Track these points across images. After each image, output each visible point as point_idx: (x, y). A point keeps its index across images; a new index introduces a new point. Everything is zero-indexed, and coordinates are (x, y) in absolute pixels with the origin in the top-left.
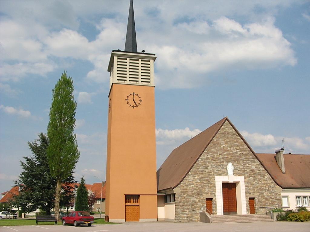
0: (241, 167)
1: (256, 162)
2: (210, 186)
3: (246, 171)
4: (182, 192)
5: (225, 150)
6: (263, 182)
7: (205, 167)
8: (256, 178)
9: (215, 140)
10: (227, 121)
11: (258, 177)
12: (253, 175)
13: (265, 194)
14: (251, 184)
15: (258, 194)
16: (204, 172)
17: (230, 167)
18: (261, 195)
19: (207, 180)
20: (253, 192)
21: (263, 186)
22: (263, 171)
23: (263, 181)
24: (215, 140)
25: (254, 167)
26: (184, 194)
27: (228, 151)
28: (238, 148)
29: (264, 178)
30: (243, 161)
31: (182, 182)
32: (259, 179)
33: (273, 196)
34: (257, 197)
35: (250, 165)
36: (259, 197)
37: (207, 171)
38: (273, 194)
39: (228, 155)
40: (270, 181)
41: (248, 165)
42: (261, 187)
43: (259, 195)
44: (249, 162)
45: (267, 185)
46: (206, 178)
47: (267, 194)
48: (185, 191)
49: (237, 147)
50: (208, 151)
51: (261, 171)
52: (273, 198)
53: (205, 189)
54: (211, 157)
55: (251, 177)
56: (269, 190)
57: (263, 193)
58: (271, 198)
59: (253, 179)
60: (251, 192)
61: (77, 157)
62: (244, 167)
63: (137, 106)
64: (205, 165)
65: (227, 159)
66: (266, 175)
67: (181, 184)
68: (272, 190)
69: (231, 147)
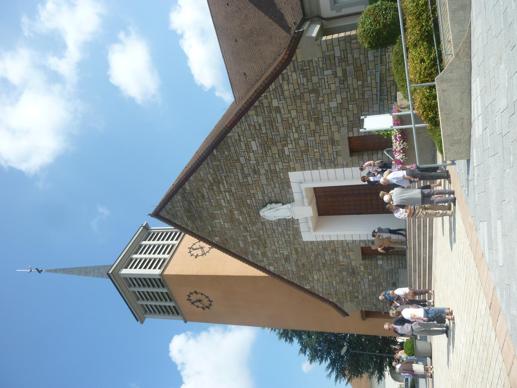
1: (237, 138)
2: (330, 252)
3: (272, 168)
4: (352, 301)
5: (232, 219)
6: (294, 113)
7: (287, 259)
8: (286, 136)
9: (217, 239)
11: (281, 129)
12: (280, 147)
13: (333, 104)
14: (306, 151)
15: (334, 128)
16: (300, 263)
17: (272, 213)
18: (339, 119)
19: (316, 256)
20: (330, 146)
21: (305, 113)
22: (257, 115)
23: (289, 112)
24: (217, 239)
25: (253, 143)
26: (357, 297)
27: (231, 212)
29: (278, 110)
30: (245, 176)
31: (331, 300)
33: (335, 74)
34: (344, 130)
35: (251, 154)
36: (345, 123)
37: (294, 256)
38: (329, 72)
39: (242, 213)
40: (286, 87)
41: (253, 162)
43: (337, 123)
44: (242, 160)
45: (301, 97)
46: (312, 258)
47: (331, 96)
48: (348, 296)
49: (213, 190)
51: (260, 120)
52: (344, 71)
53: (338, 261)
54: (258, 249)
55: (287, 153)
56: (315, 91)
57: (329, 109)
59: (290, 146)
60: (330, 151)
62: (262, 171)
64: (283, 262)
65: (252, 214)
66: (270, 103)
67: (335, 300)
68: (315, 79)
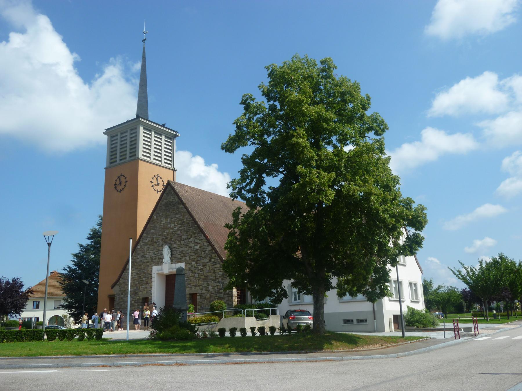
0: (182, 249)
1: (201, 238)
2: (147, 281)
3: (187, 255)
4: (120, 291)
5: (165, 228)
6: (208, 268)
7: (143, 256)
8: (199, 263)
9: (155, 217)
10: (169, 187)
11: (203, 261)
12: (195, 260)
13: (210, 287)
14: (193, 273)
15: (201, 287)
16: (141, 263)
17: (166, 251)
18: (204, 289)
19: (144, 273)
20: (194, 284)
21: (208, 274)
22: (209, 251)
23: (209, 266)
24: (155, 217)
25: (198, 246)
26: (122, 294)
27: (168, 229)
28: (180, 222)
29: (210, 261)
30: (184, 239)
31: (121, 279)
32: (204, 265)
33: (221, 289)
34: (200, 292)
35: (193, 245)
36: (203, 292)
37: (145, 261)
38: (222, 287)
39: (167, 234)
40: (218, 266)
41: (190, 245)
42: (206, 276)
43: (203, 288)
44: (191, 239)
45: (214, 273)
46: (143, 271)
47: (213, 286)
48: (123, 289)
49: (179, 220)
50: (147, 233)
51: (207, 252)
52: (221, 293)
53: (142, 285)
54: (149, 241)
55: (193, 263)
56: (215, 280)
57: (208, 285)
58: (219, 293)
59: (195, 265)
60: (192, 284)
61: (426, 222)
62: (186, 249)
63: (153, 186)
64: (142, 254)
65: (167, 240)
66: (213, 258)
67: (120, 281)
68: (220, 280)
69: (171, 222)
